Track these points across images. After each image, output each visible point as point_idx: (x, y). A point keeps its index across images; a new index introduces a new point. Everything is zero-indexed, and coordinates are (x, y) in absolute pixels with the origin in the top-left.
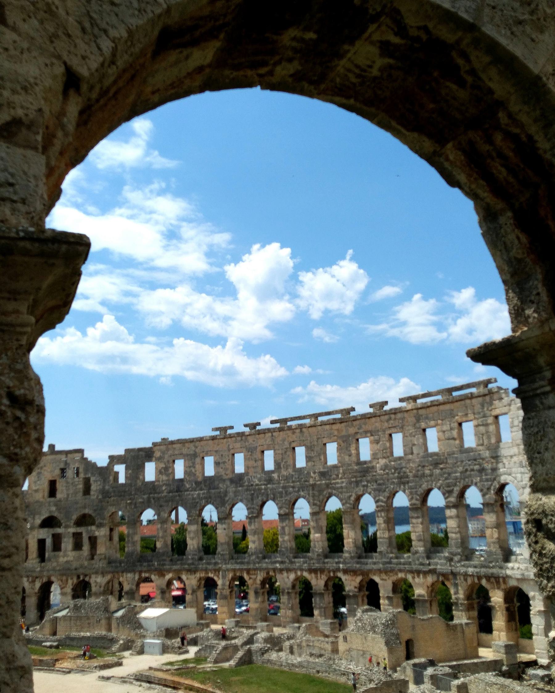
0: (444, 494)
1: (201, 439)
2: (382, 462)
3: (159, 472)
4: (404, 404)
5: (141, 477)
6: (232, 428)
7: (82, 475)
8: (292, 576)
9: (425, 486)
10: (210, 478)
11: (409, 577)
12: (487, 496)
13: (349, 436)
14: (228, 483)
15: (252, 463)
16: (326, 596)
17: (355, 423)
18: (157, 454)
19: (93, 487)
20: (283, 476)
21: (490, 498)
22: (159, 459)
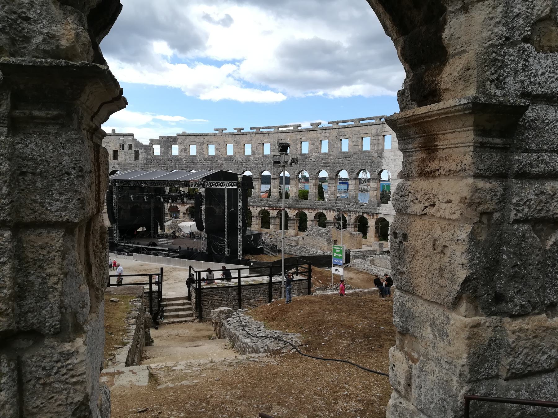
0: (349, 173)
1: (206, 135)
2: (315, 154)
3: (181, 151)
4: (331, 125)
5: (170, 153)
6: (226, 129)
7: (133, 148)
8: (259, 209)
9: (338, 169)
10: (212, 157)
11: (325, 212)
12: (373, 175)
13: (297, 140)
14: (223, 160)
15: (238, 150)
16: (277, 219)
17: (301, 133)
18: (180, 140)
19: (141, 156)
20: (257, 158)
21: (374, 176)
22: (181, 144)
